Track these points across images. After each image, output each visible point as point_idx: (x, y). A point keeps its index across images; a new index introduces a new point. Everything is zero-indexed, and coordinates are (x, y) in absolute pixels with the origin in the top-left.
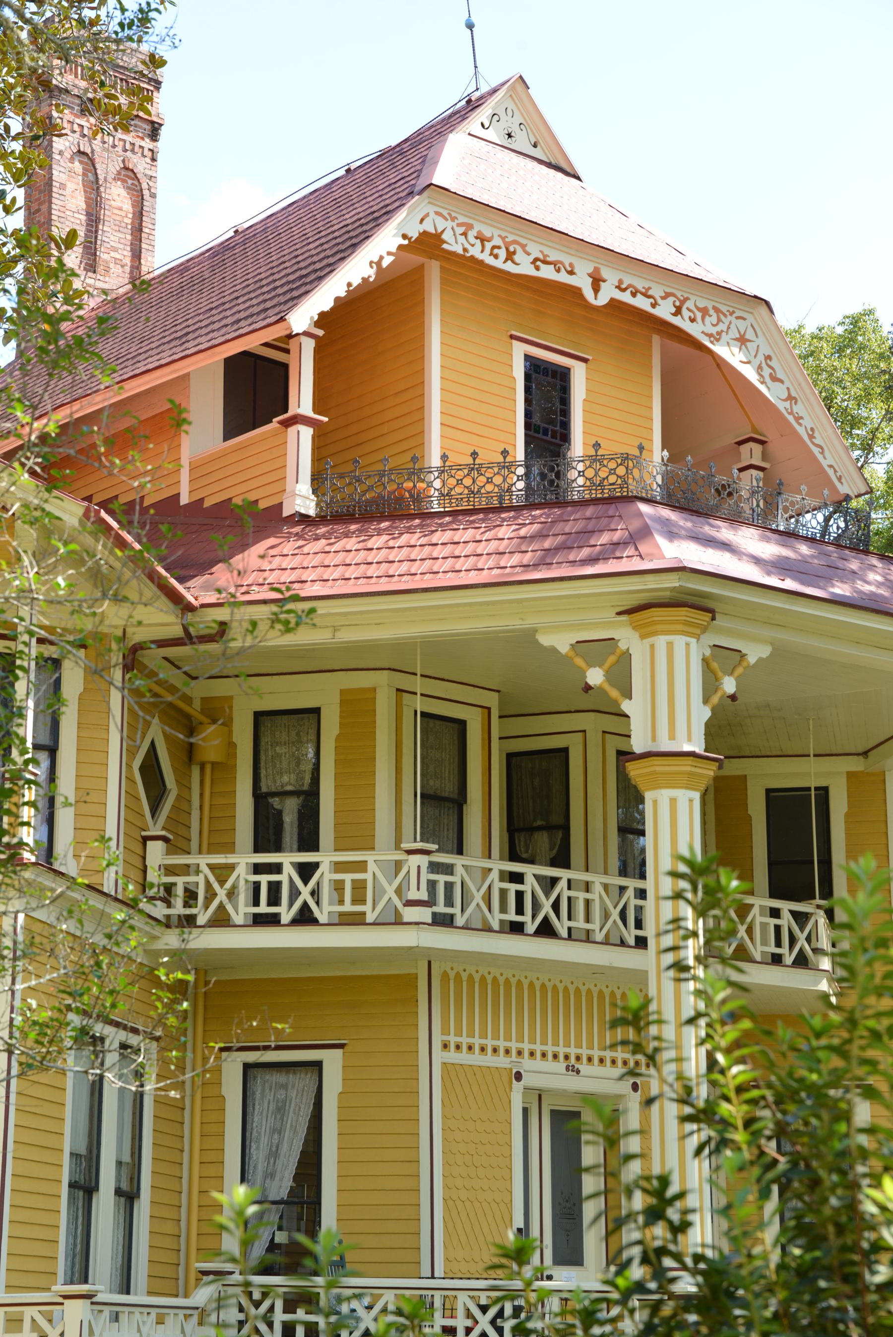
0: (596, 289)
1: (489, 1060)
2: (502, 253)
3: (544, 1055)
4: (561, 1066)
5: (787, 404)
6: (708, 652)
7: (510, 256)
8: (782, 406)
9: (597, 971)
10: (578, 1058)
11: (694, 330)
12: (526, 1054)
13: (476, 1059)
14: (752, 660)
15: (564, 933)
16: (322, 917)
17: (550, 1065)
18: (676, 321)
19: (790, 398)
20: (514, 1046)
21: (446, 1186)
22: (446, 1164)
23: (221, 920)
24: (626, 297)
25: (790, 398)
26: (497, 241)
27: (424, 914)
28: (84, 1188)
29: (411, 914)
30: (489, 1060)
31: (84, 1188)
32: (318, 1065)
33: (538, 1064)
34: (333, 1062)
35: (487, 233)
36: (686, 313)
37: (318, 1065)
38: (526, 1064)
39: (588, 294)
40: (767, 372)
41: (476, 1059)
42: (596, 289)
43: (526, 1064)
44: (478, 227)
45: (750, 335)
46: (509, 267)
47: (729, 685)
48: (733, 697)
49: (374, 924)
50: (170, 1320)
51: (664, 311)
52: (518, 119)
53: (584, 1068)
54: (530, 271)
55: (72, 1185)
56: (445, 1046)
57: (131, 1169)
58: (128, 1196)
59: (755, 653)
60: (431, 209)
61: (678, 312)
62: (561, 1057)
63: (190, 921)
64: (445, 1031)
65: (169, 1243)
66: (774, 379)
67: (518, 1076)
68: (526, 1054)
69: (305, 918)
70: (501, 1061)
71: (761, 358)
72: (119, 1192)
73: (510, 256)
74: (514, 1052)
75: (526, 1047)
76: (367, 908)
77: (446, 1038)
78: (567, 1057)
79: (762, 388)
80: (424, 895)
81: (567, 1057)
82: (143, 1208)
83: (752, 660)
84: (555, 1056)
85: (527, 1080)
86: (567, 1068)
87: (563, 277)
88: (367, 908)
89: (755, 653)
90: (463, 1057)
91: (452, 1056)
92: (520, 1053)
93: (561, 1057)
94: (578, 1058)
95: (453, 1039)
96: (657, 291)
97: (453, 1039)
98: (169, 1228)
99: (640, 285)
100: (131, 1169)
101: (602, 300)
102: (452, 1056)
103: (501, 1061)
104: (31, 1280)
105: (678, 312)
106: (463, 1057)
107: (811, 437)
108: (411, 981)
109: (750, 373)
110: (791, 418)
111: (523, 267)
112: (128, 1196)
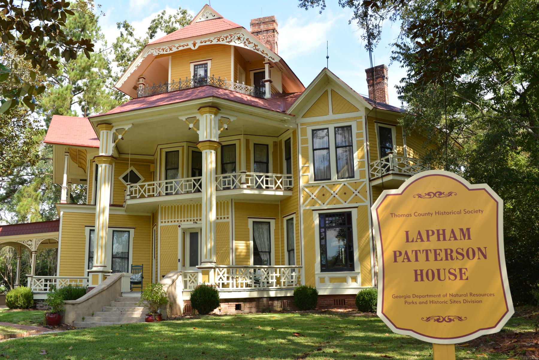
0: (194, 45)
1: (173, 224)
2: (169, 50)
4: (192, 222)
5: (254, 48)
6: (115, 131)
7: (171, 49)
8: (252, 49)
9: (191, 200)
10: (197, 220)
11: (224, 43)
14: (126, 129)
17: (189, 222)
18: (219, 43)
19: (255, 45)
24: (204, 44)
25: (255, 45)
26: (167, 48)
30: (173, 224)
33: (186, 223)
35: (164, 47)
36: (221, 40)
39: (193, 48)
40: (247, 42)
42: (194, 45)
43: (183, 223)
44: (162, 48)
45: (242, 36)
46: (171, 52)
47: (120, 137)
48: (122, 139)
51: (215, 42)
52: (209, 13)
53: (198, 222)
54: (177, 50)
59: (127, 128)
60: (150, 50)
61: (219, 40)
64: (162, 219)
66: (249, 43)
67: (179, 226)
70: (176, 223)
71: (245, 40)
73: (171, 49)
75: (183, 219)
79: (246, 47)
80: (129, 193)
83: (126, 129)
85: (182, 227)
87: (186, 47)
89: (127, 128)
90: (167, 224)
91: (163, 224)
94: (197, 220)
95: (163, 221)
96: (212, 39)
99: (207, 39)
101: (197, 47)
102: (163, 224)
103: (176, 223)
105: (219, 40)
106: (167, 224)
107: (262, 53)
109: (242, 45)
110: (256, 51)
111: (175, 50)
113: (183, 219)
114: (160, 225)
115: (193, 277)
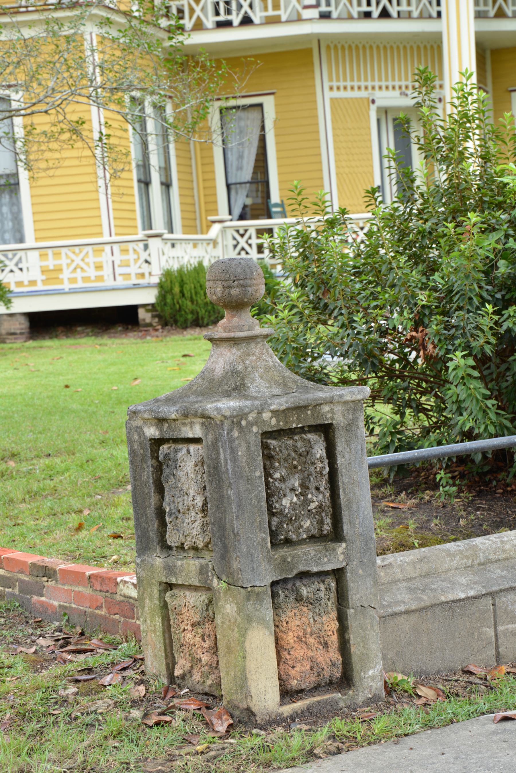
1: (356, 94)
3: (387, 88)
4: (397, 93)
10: (407, 87)
12: (377, 88)
13: (349, 94)
15: (394, 14)
16: (256, 20)
17: (391, 93)
20: (370, 84)
21: (337, 167)
22: (336, 154)
23: (199, 26)
27: (314, 13)
28: (145, 183)
29: (307, 14)
30: (356, 94)
31: (145, 183)
32: (260, 106)
33: (384, 93)
34: (269, 104)
37: (260, 106)
38: (378, 94)
41: (349, 94)
49: (287, 21)
50: (200, 246)
55: (139, 181)
56: (331, 88)
57: (166, 170)
58: (167, 185)
62: (397, 88)
63: (181, 29)
64: (330, 79)
65: (190, 208)
67: (373, 101)
68: (377, 88)
69: (247, 21)
70: (363, 94)
72: (162, 184)
74: (370, 88)
75: (377, 84)
76: (281, 12)
77: (331, 84)
78: (400, 87)
81: (400, 87)
82: (175, 190)
84: (394, 88)
86: (401, 94)
88: (281, 12)
90: (342, 94)
91: (335, 94)
92: (373, 88)
93: (397, 88)
94: (407, 87)
95: (335, 84)
97: (335, 84)
98: (189, 200)
100: (166, 170)
102: (335, 94)
103: (363, 94)
104: (126, 230)
106: (342, 94)
108: (308, 52)
112: (167, 185)
113: (377, 84)
114: (328, 94)
115: (242, 236)
